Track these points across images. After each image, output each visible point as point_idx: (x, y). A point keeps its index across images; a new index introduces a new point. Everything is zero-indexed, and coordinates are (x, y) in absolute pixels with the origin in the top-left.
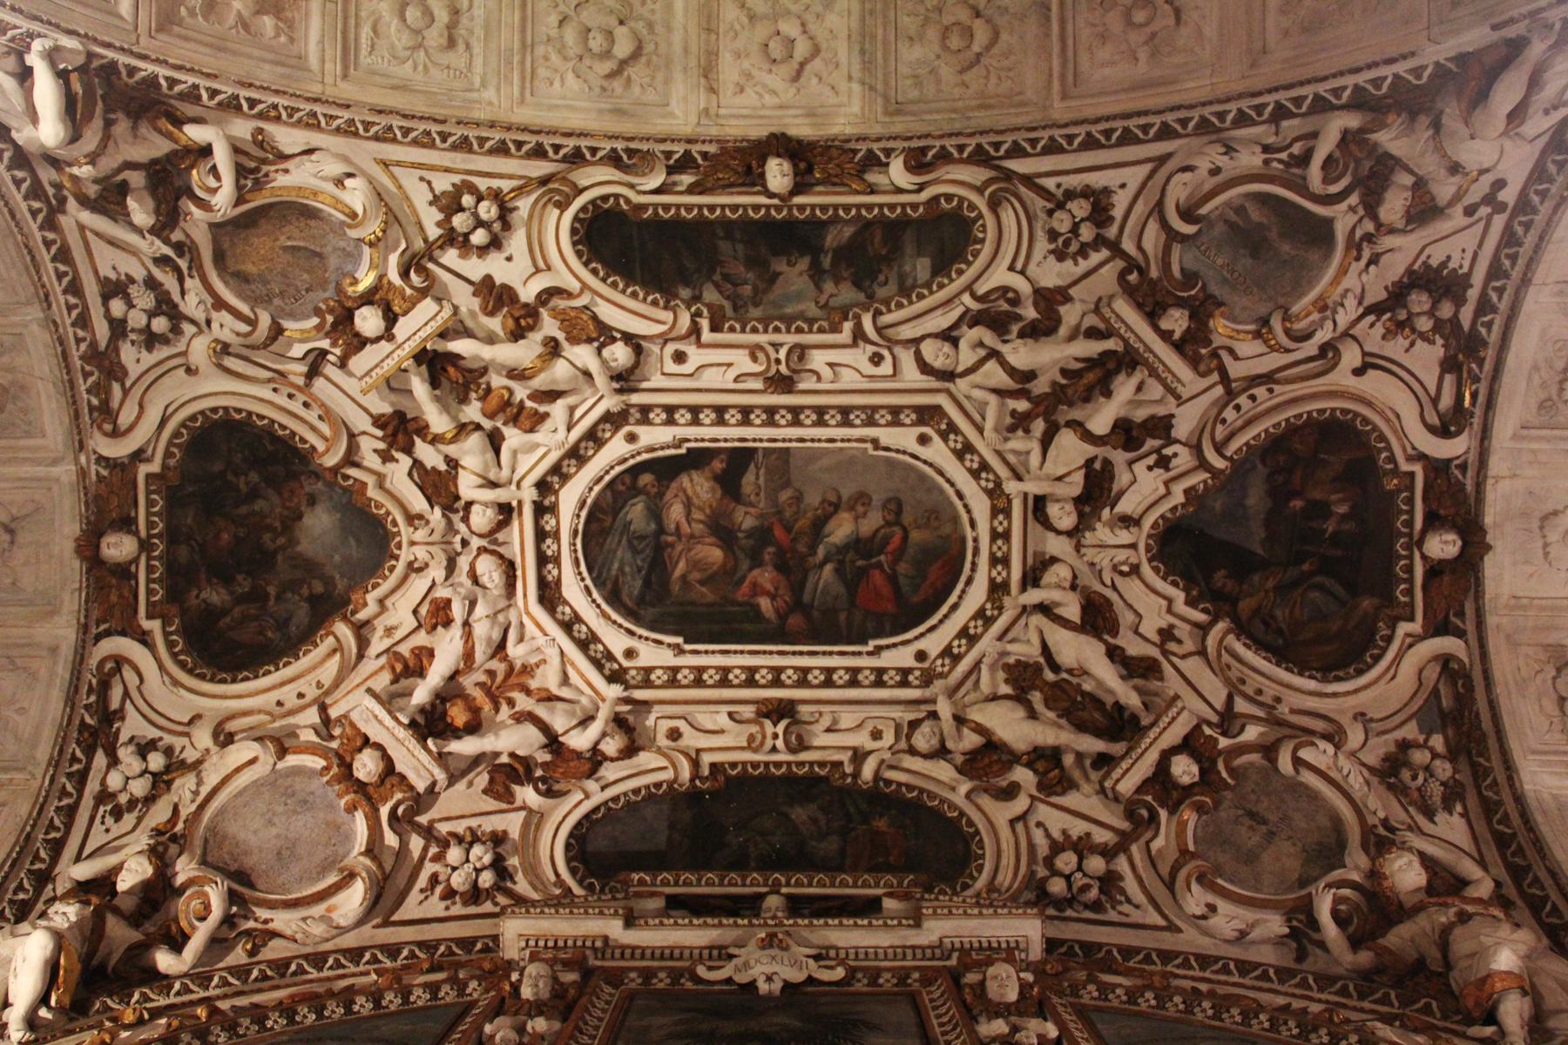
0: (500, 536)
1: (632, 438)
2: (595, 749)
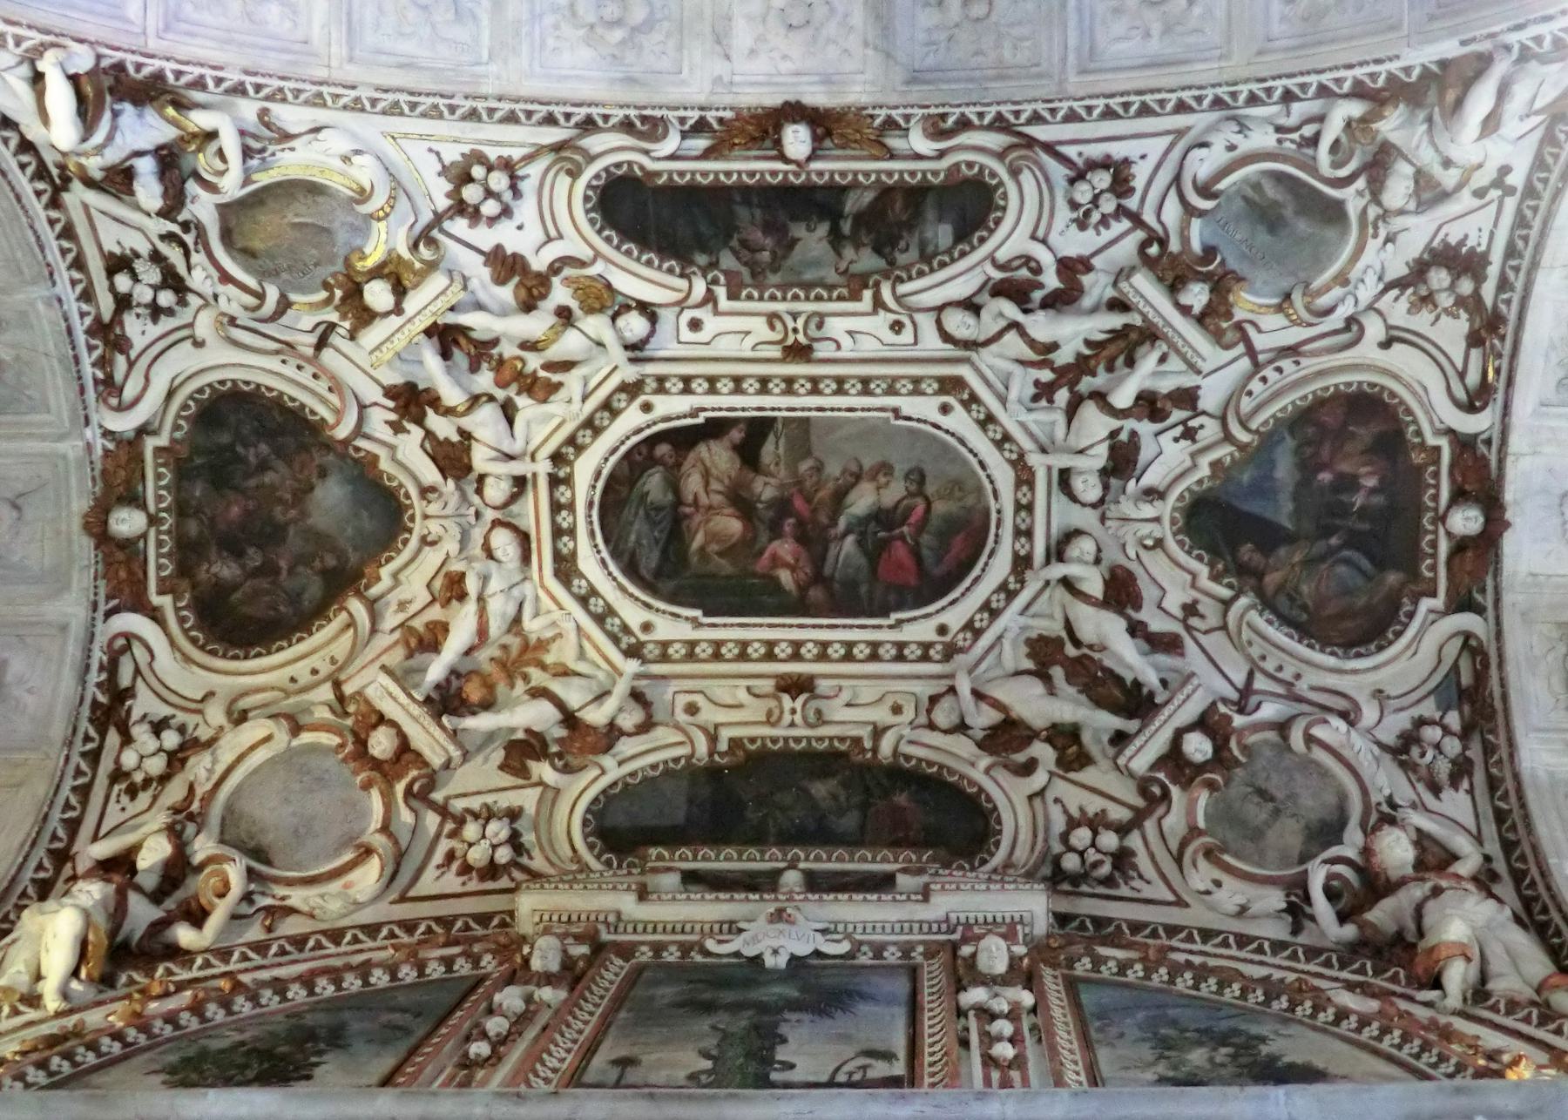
0: (514, 508)
1: (647, 407)
2: (612, 725)
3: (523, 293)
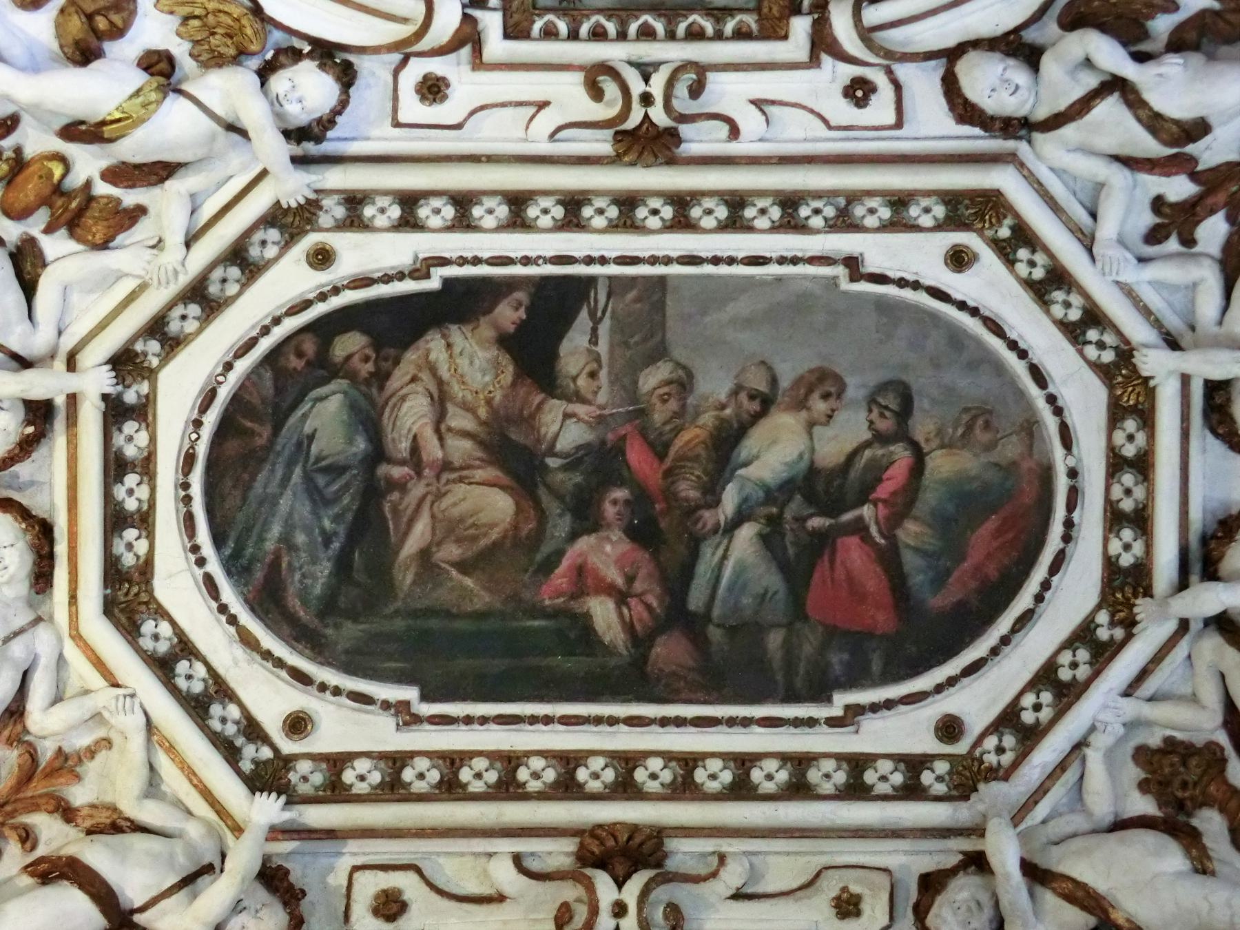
0: (23, 470)
1: (322, 258)
3: (76, 24)
